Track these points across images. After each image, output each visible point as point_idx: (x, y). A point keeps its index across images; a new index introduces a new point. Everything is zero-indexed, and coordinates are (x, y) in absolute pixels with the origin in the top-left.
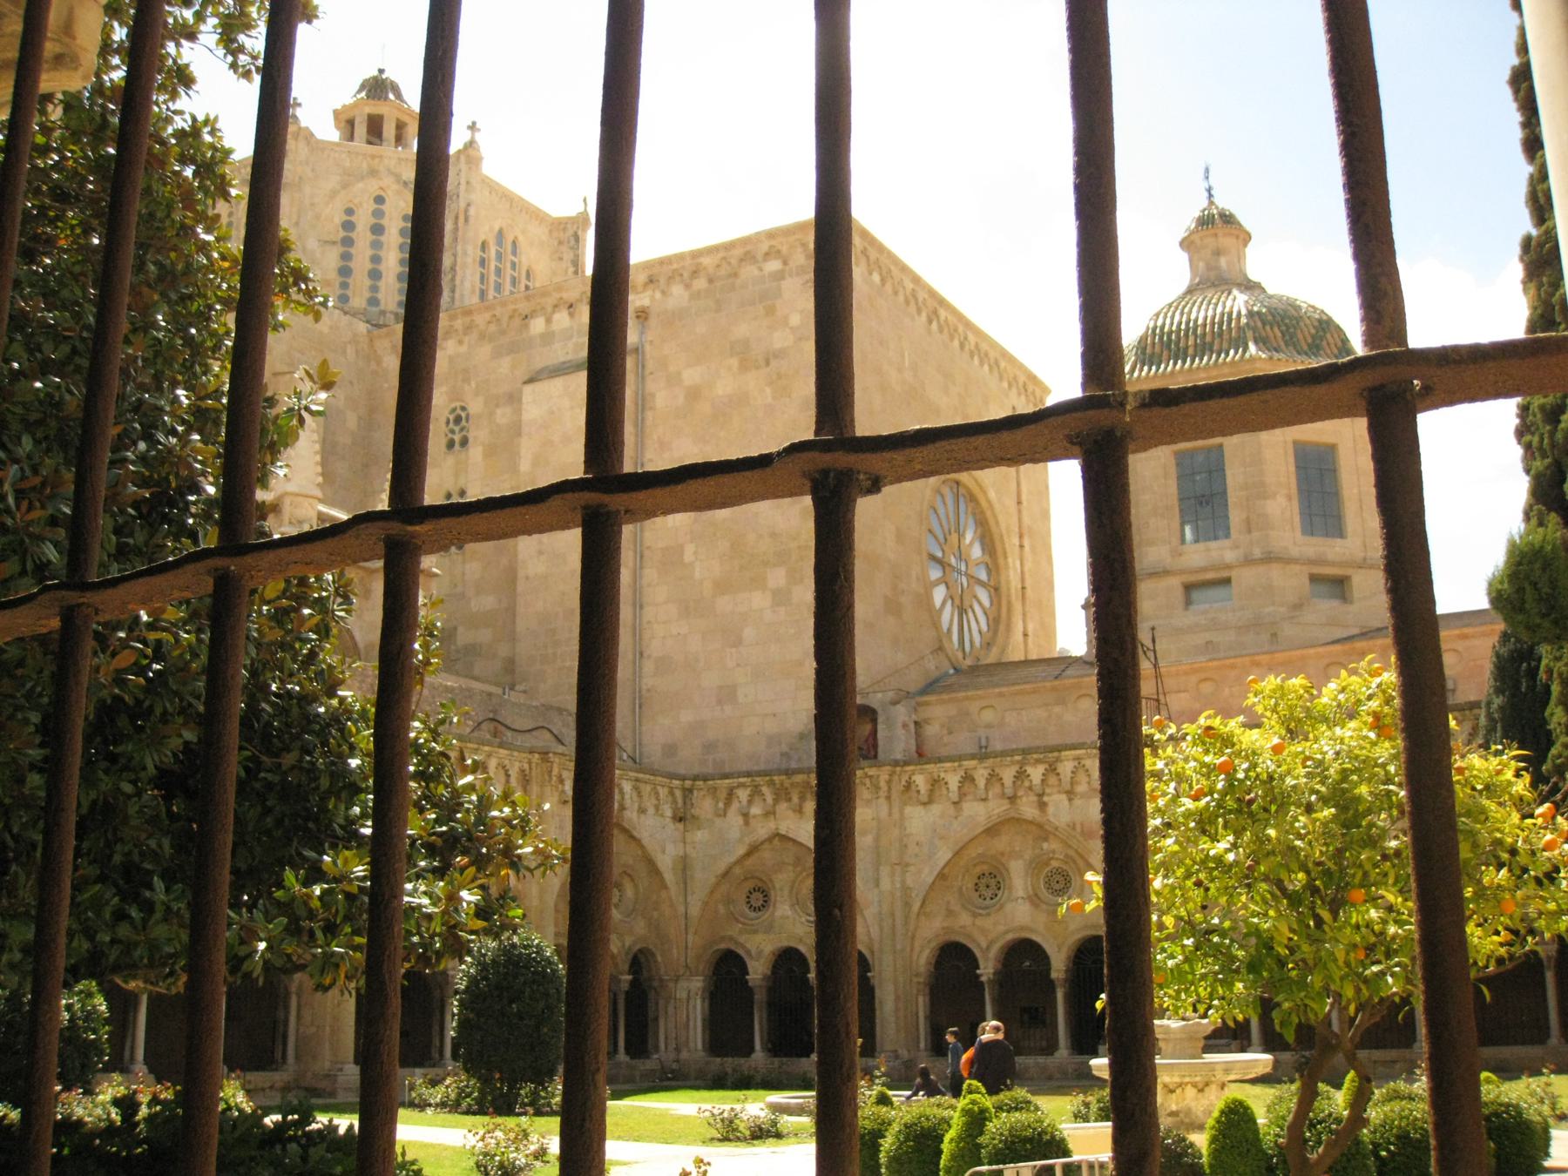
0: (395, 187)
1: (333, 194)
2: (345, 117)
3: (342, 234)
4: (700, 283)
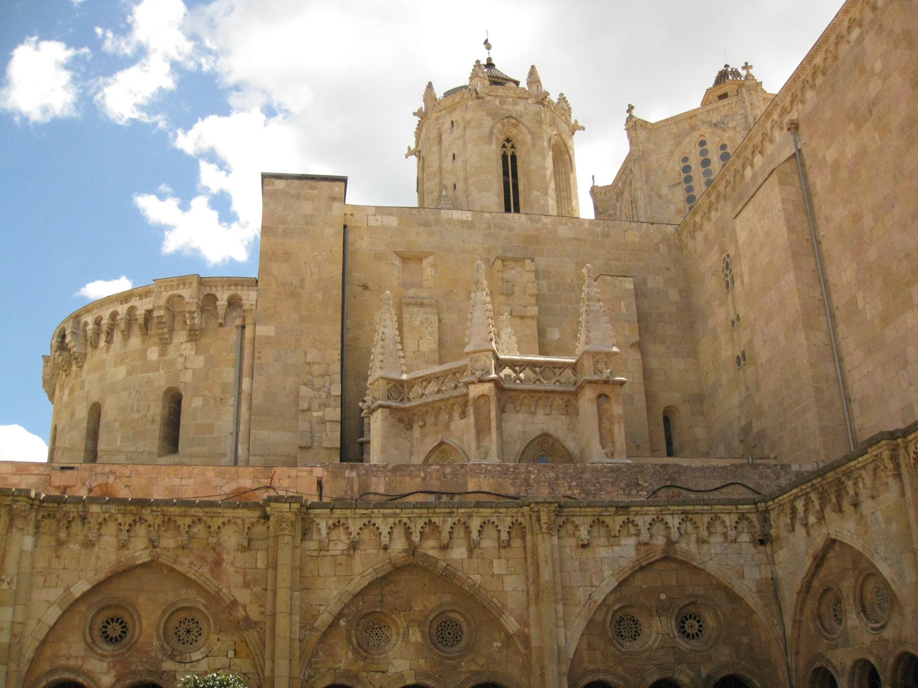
0: (710, 130)
1: (672, 153)
3: (683, 176)
4: (820, 80)
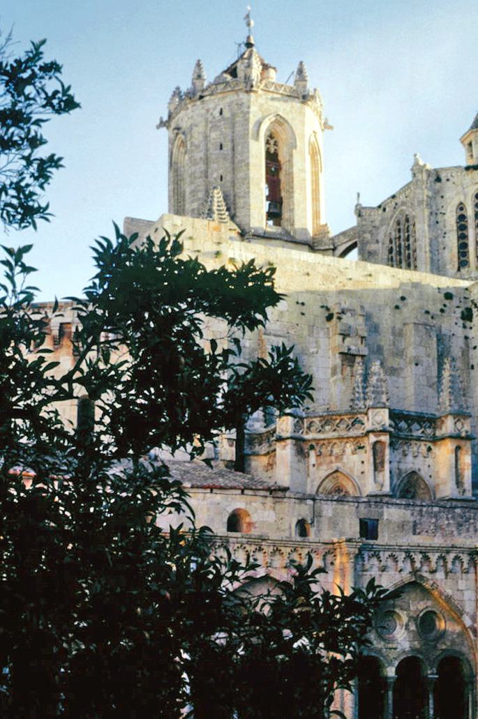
2: (467, 142)
